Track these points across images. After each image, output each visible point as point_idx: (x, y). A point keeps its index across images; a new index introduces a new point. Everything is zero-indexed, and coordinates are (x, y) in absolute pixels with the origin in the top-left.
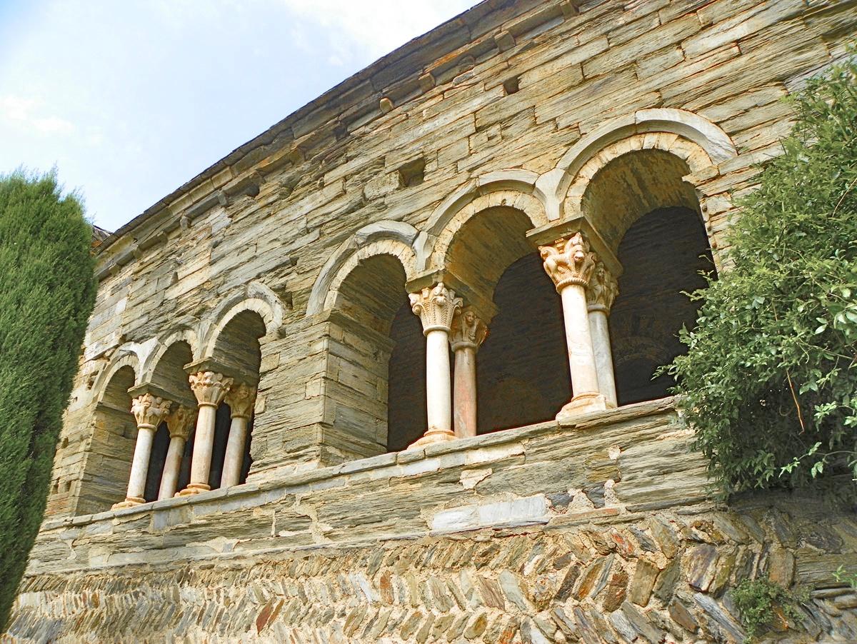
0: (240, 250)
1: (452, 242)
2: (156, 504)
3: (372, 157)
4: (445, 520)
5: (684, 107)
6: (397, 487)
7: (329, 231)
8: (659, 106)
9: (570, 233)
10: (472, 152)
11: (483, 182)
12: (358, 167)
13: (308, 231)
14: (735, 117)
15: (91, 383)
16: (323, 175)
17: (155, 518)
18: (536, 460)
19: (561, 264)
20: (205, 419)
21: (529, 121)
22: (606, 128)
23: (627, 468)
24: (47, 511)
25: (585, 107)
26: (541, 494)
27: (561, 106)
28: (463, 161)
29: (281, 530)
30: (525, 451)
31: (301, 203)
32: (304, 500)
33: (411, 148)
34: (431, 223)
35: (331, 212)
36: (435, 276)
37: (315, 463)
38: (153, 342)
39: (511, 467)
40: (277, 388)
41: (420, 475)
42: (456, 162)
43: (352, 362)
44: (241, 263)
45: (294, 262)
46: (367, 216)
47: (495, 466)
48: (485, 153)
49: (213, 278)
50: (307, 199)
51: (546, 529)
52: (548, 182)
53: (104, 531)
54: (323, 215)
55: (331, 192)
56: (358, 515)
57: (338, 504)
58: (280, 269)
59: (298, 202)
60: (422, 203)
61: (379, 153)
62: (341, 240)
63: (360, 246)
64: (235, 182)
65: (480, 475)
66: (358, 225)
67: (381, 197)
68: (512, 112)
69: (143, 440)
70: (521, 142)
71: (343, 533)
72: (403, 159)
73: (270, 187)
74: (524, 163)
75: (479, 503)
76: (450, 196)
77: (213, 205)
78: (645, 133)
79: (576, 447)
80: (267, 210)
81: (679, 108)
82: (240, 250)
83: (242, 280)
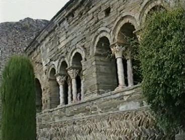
0: (72, 34)
1: (119, 33)
2: (67, 105)
4: (122, 108)
13: (87, 29)
15: (46, 73)
17: (67, 109)
20: (74, 82)
24: (43, 108)
31: (84, 20)
32: (95, 104)
34: (113, 28)
37: (96, 94)
38: (57, 61)
40: (87, 75)
43: (104, 65)
45: (85, 38)
47: (130, 95)
49: (68, 43)
50: (86, 19)
51: (136, 111)
52: (137, 17)
53: (56, 113)
55: (91, 17)
56: (105, 107)
62: (94, 32)
63: (99, 34)
64: (67, 14)
65: (127, 97)
69: (61, 88)
73: (77, 13)
77: (64, 19)
80: (77, 22)
82: (72, 34)
83: (74, 44)
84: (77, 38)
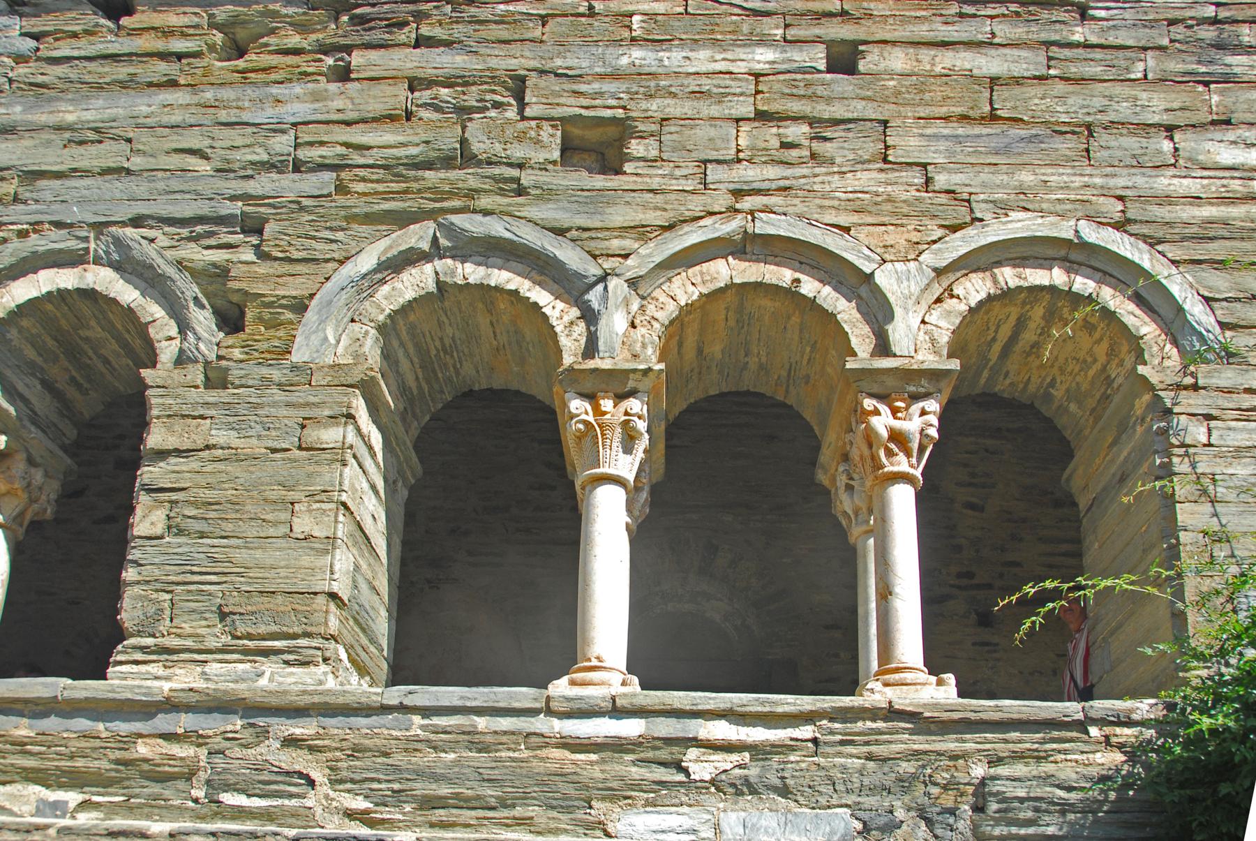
3: (493, 62)
5: (1159, 248)
6: (543, 753)
7: (360, 187)
8: (1120, 226)
9: (922, 390)
10: (741, 155)
11: (760, 228)
12: (453, 72)
14: (1238, 300)
16: (349, 49)
18: (840, 754)
19: (898, 437)
21: (872, 147)
22: (1020, 225)
23: (998, 793)
25: (987, 169)
26: (845, 810)
27: (943, 145)
28: (720, 167)
29: (226, 791)
30: (818, 735)
33: (596, 86)
35: (369, 148)
36: (638, 376)
39: (792, 758)
41: (599, 740)
42: (705, 162)
44: (75, 170)
46: (472, 193)
47: (758, 751)
48: (772, 172)
54: (347, 145)
57: (390, 761)
58: (207, 228)
59: (267, 84)
60: (619, 216)
61: (513, 63)
62: (403, 220)
66: (446, 204)
67: (510, 165)
68: (838, 111)
70: (852, 182)
71: (400, 817)
72: (572, 101)
74: (856, 225)
75: (721, 805)
76: (686, 228)
78: (1080, 264)
79: (916, 747)
81: (1151, 245)
82: (75, 136)
84: (117, 187)
